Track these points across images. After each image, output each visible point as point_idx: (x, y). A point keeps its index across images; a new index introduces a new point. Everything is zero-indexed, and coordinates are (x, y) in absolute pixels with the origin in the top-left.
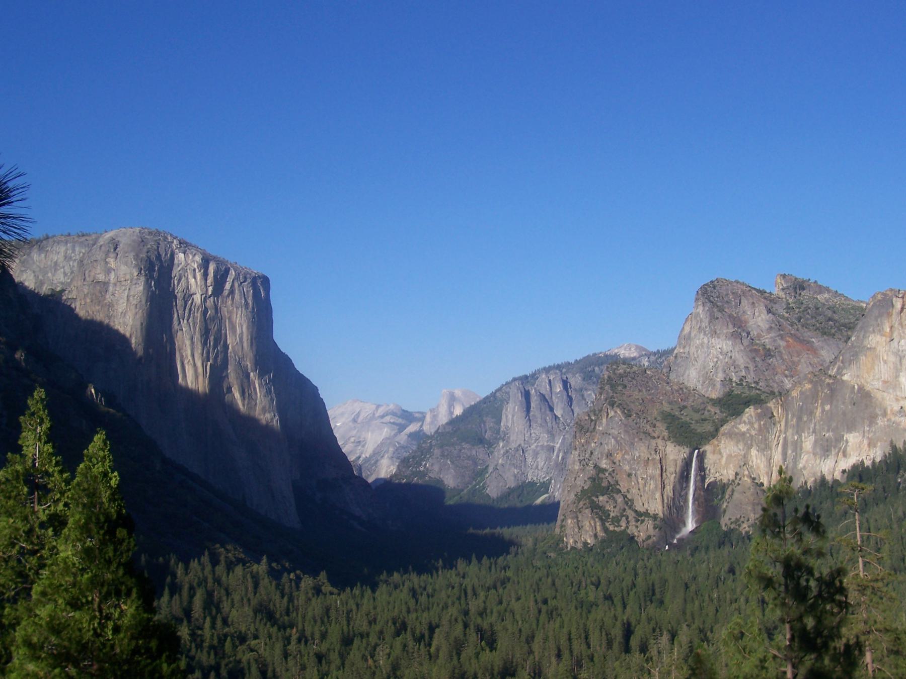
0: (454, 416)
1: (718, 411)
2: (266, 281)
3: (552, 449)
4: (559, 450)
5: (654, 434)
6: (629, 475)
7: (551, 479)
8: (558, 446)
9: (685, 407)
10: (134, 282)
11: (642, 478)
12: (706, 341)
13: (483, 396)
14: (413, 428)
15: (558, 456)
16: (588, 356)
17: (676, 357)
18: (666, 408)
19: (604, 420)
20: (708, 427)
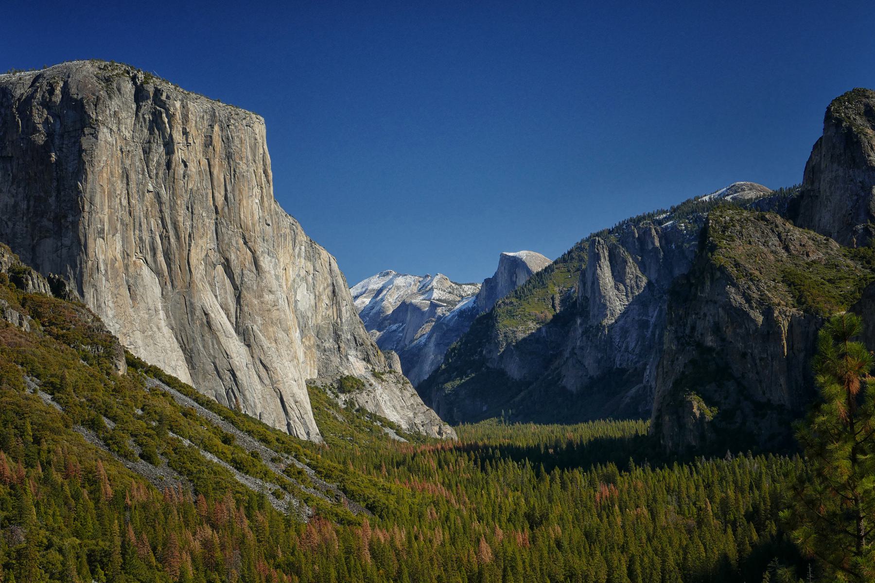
1: (859, 267)
3: (644, 325)
4: (655, 326)
5: (776, 301)
6: (744, 355)
7: (646, 364)
8: (653, 320)
9: (814, 262)
10: (86, 132)
11: (761, 359)
12: (841, 173)
15: (653, 334)
17: (802, 195)
18: (790, 266)
19: (708, 283)
20: (849, 287)
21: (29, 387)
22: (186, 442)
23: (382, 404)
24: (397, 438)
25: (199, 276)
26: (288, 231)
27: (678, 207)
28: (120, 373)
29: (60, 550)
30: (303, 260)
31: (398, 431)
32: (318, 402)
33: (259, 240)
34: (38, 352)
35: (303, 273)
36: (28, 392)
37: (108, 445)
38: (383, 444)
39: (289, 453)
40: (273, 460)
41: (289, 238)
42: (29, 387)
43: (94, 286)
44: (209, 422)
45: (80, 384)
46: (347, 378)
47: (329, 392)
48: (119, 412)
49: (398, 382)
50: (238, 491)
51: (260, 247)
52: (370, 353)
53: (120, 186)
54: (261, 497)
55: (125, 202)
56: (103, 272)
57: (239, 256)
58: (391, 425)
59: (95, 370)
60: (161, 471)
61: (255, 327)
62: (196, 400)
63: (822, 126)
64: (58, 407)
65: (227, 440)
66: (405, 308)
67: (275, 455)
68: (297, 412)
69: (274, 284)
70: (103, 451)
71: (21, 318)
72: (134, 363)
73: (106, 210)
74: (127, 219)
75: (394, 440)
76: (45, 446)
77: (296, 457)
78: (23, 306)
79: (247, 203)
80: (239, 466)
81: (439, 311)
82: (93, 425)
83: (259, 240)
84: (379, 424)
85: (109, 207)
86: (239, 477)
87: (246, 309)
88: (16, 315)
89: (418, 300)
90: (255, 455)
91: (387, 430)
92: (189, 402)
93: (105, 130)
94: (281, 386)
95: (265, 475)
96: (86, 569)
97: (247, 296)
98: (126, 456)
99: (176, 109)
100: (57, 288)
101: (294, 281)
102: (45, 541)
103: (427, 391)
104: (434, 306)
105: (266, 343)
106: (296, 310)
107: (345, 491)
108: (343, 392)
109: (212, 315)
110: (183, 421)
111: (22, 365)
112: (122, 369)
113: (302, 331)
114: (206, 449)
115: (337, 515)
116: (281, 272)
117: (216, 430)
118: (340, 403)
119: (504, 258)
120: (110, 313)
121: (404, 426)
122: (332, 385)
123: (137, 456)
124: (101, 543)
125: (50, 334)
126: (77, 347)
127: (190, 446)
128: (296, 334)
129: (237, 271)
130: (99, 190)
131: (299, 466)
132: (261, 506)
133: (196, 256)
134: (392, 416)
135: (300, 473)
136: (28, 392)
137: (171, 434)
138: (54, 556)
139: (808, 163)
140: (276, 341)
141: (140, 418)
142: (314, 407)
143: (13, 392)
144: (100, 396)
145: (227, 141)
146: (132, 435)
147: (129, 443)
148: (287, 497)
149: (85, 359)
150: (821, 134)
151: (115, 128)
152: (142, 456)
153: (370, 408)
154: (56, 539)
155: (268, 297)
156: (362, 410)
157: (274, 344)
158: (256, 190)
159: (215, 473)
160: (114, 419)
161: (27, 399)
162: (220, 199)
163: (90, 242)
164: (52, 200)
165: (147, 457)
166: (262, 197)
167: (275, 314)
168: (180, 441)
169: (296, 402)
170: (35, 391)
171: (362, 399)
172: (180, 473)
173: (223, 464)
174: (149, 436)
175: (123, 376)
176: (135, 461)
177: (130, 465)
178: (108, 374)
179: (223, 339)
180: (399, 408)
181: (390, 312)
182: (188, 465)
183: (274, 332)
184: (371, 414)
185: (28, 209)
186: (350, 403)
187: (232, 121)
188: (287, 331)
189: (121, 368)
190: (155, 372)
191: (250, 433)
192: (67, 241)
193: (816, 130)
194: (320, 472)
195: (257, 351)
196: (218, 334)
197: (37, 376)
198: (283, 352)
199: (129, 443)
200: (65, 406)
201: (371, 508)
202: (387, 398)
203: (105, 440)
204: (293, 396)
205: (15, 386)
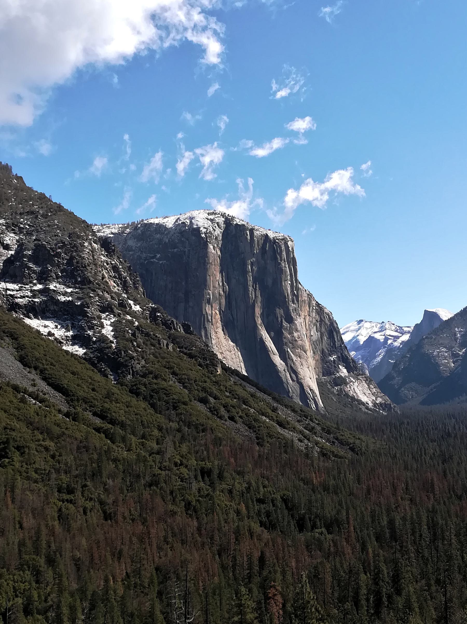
21: (172, 380)
22: (252, 410)
23: (357, 391)
24: (366, 410)
25: (259, 322)
26: (306, 298)
28: (218, 373)
29: (186, 467)
30: (314, 314)
31: (367, 408)
33: (291, 303)
34: (176, 361)
35: (314, 321)
36: (171, 383)
37: (211, 411)
39: (307, 418)
40: (299, 421)
41: (307, 302)
42: (172, 380)
43: (205, 328)
44: (264, 400)
45: (197, 379)
46: (339, 377)
47: (329, 385)
48: (218, 394)
49: (367, 380)
50: (279, 437)
51: (292, 306)
52: (351, 364)
53: (218, 277)
54: (292, 441)
55: (221, 284)
56: (210, 320)
57: (280, 312)
58: (363, 404)
59: (205, 371)
60: (240, 426)
61: (289, 350)
64: (186, 391)
66: (371, 340)
67: (299, 418)
68: (311, 395)
69: (299, 328)
70: (209, 414)
71: (167, 345)
72: (226, 369)
73: (212, 288)
74: (222, 292)
75: (365, 412)
76: (179, 411)
77: (311, 420)
78: (169, 337)
79: (285, 284)
80: (281, 424)
81: (389, 342)
82: (204, 401)
83: (291, 303)
84: (356, 403)
85: (214, 287)
86: (279, 429)
87: (284, 340)
88: (165, 342)
89: (379, 337)
91: (362, 407)
93: (212, 247)
94: (302, 381)
95: (294, 429)
96: (200, 478)
97: (286, 334)
98: (221, 418)
99: (247, 235)
100: (187, 328)
101: (309, 325)
102: (179, 462)
103: (383, 385)
104: (386, 339)
105: (294, 358)
106: (310, 340)
107: (337, 439)
108: (337, 385)
109: (266, 343)
110: (251, 399)
111: (168, 368)
112: (219, 371)
113: (314, 353)
114: (263, 414)
115: (333, 452)
116: (302, 320)
117: (268, 405)
118: (335, 391)
119: (427, 313)
120: (214, 342)
121: (371, 405)
122: (330, 381)
123: (227, 418)
124: (207, 463)
125: (182, 352)
126: (196, 360)
127: (254, 413)
128: (310, 353)
129: (279, 319)
130: (208, 277)
131: (312, 424)
132: (292, 446)
133: (258, 311)
134: (364, 399)
135: (313, 428)
136: (171, 383)
137: (244, 406)
138: (184, 470)
140: (300, 357)
141: (228, 397)
143: (163, 382)
144: (207, 385)
145: (275, 252)
146: (224, 407)
147: (223, 411)
148: (306, 441)
149: (200, 365)
151: (215, 245)
152: (229, 417)
153: (351, 393)
154: (184, 461)
155: (296, 334)
156: (347, 395)
157: (299, 359)
158: (289, 277)
160: (215, 398)
161: (171, 386)
162: (270, 282)
163: (204, 304)
164: (183, 283)
165: (232, 418)
166: (292, 281)
167: (300, 342)
168: (249, 410)
169: (311, 390)
170: (174, 382)
171: (347, 389)
172: (250, 428)
173: (272, 422)
174: (233, 407)
175: (219, 374)
176: (226, 421)
177: (223, 422)
178: (212, 374)
179: (272, 356)
180: (367, 395)
181: (362, 343)
183: (298, 352)
184: (352, 397)
185: (172, 288)
186: (341, 391)
187: (277, 241)
188: (305, 352)
189: (219, 370)
190: (236, 373)
191: (286, 406)
192: (191, 304)
194: (323, 429)
195: (289, 362)
196: (269, 353)
197: (176, 375)
198: (304, 363)
199: (223, 411)
200: (190, 390)
201: (352, 449)
202: (361, 389)
203: (210, 408)
204: (309, 387)
205: (165, 380)
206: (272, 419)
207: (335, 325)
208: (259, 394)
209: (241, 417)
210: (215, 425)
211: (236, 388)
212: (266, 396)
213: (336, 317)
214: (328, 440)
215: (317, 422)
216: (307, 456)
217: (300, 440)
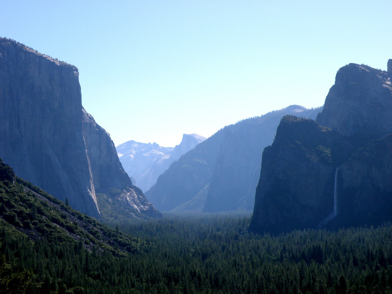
0: (190, 150)
2: (77, 70)
13: (207, 138)
14: (167, 157)
16: (270, 113)
24: (135, 216)
27: (265, 115)
32: (100, 200)
38: (130, 219)
54: (80, 244)
58: (135, 211)
62: (49, 198)
63: (335, 80)
65: (64, 217)
72: (18, 181)
80: (70, 230)
84: (128, 210)
90: (76, 224)
92: (44, 199)
98: (17, 225)
110: (42, 208)
131: (96, 229)
139: (327, 97)
142: (97, 202)
148: (91, 243)
150: (334, 84)
159: (58, 232)
182: (45, 228)
193: (332, 82)
194: (104, 233)
201: (129, 250)
206: (62, 225)
207: (112, 145)
208: (50, 204)
209: (35, 224)
210: (10, 231)
211: (30, 198)
212: (55, 205)
213: (113, 138)
214: (109, 243)
215: (99, 227)
216: (94, 255)
217: (86, 243)
